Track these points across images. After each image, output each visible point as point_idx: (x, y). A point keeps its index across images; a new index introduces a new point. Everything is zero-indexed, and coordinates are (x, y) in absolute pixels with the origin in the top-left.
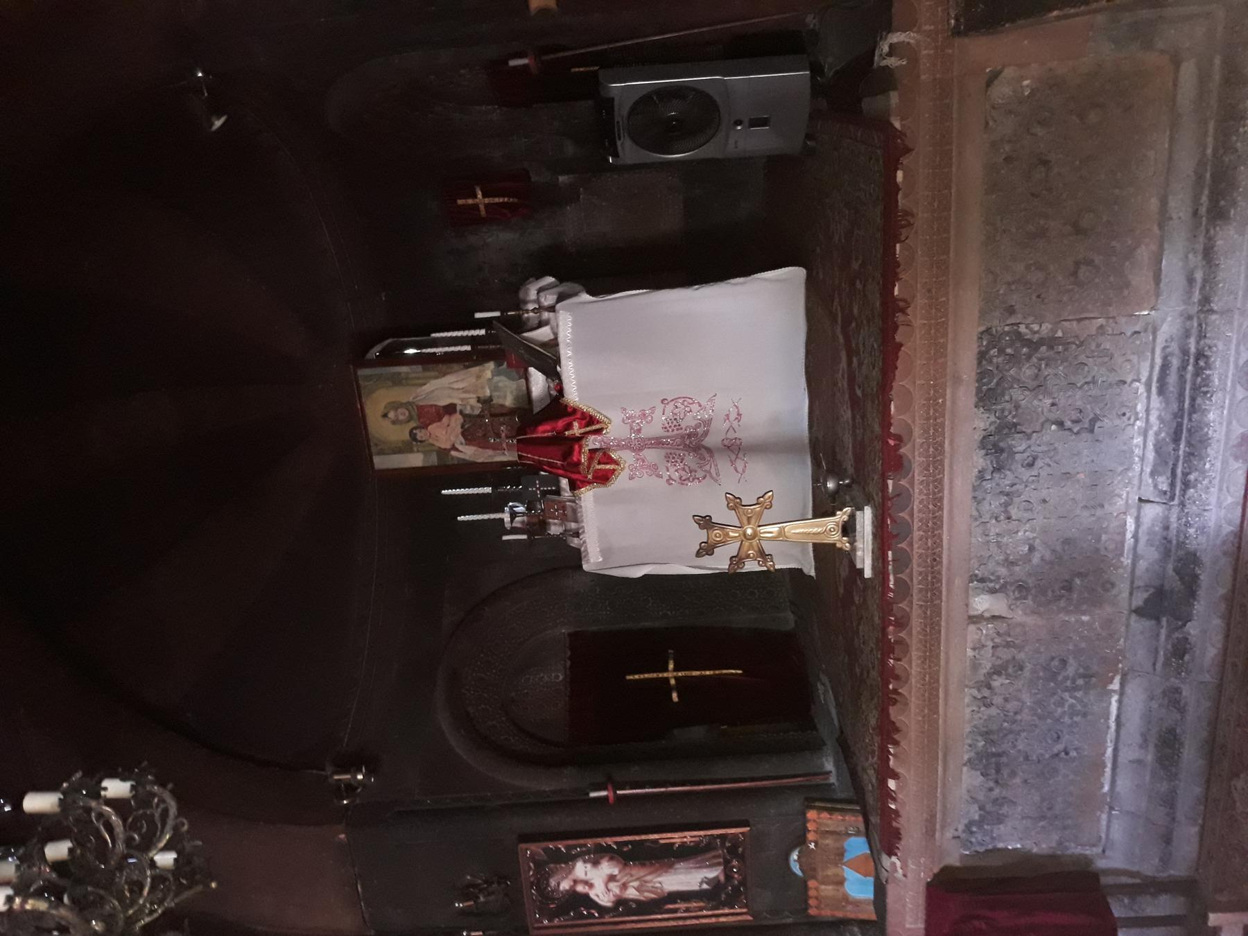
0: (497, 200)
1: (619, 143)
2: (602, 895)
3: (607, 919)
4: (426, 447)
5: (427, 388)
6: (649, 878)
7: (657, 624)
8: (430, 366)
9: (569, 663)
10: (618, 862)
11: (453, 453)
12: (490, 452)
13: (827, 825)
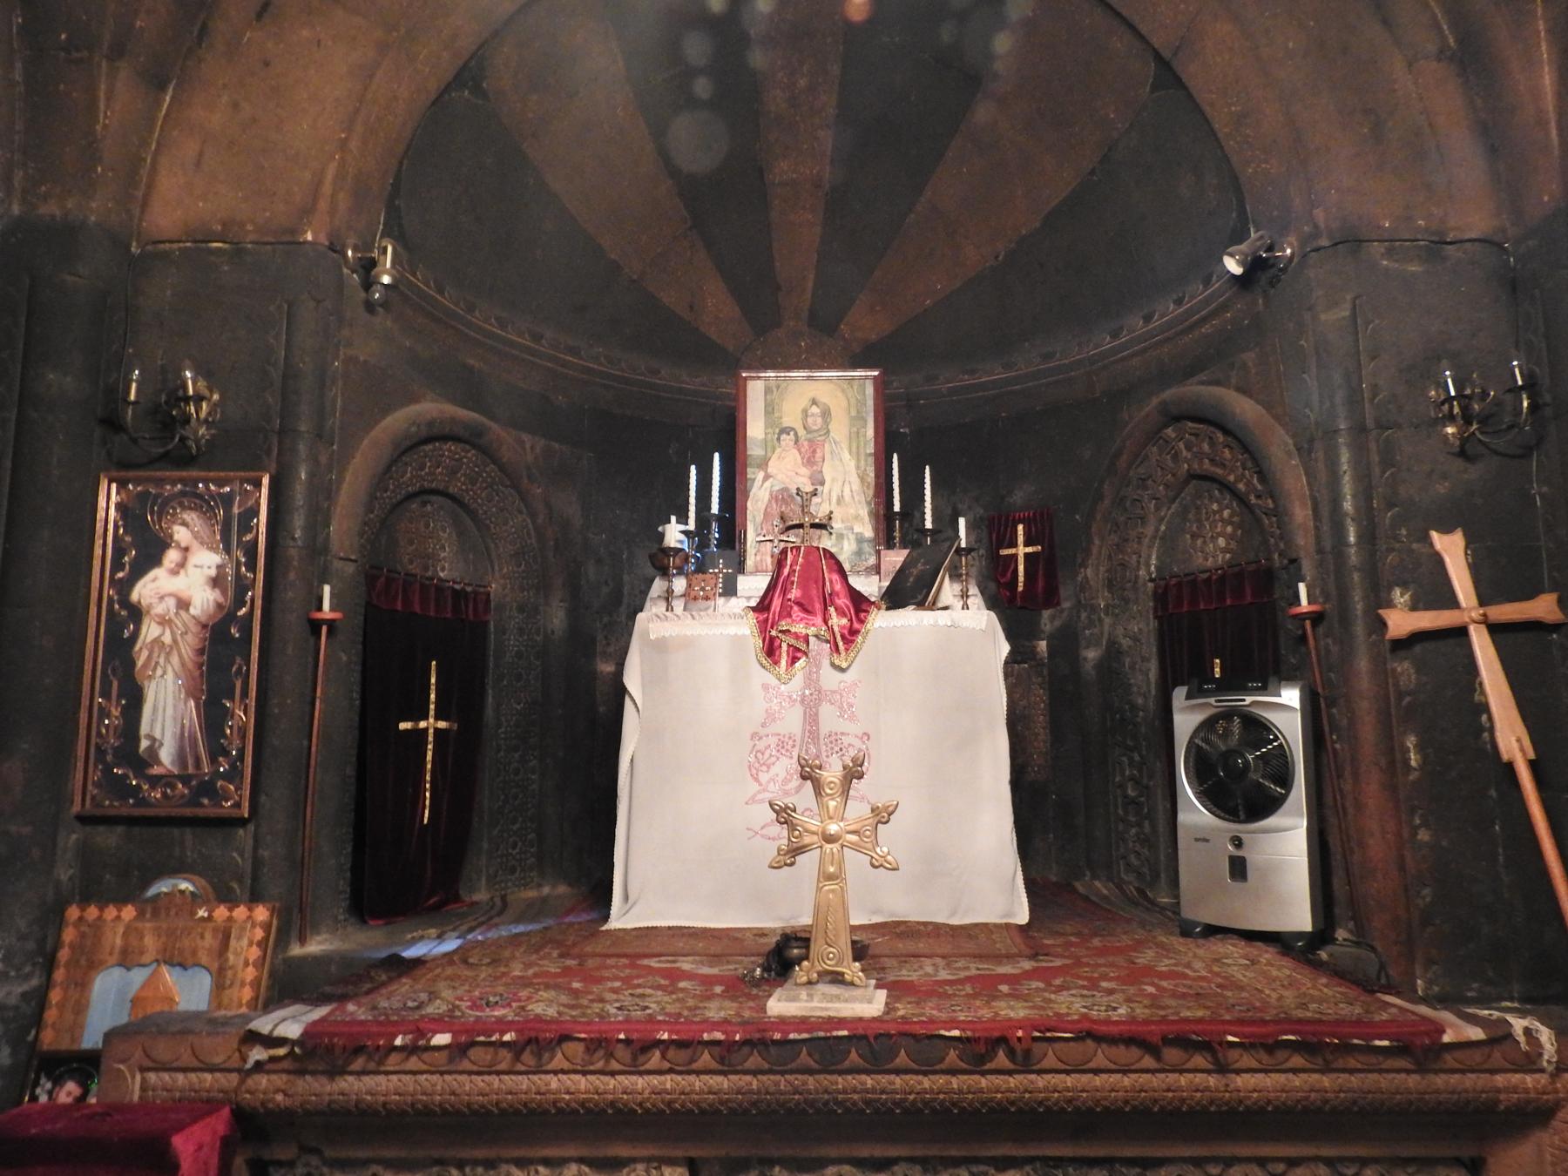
0: (1021, 568)
1: (1212, 700)
2: (153, 588)
3: (109, 592)
4: (769, 446)
5: (846, 456)
6: (175, 659)
7: (489, 712)
8: (871, 460)
9: (457, 587)
10: (210, 617)
11: (761, 475)
12: (760, 518)
13: (239, 938)
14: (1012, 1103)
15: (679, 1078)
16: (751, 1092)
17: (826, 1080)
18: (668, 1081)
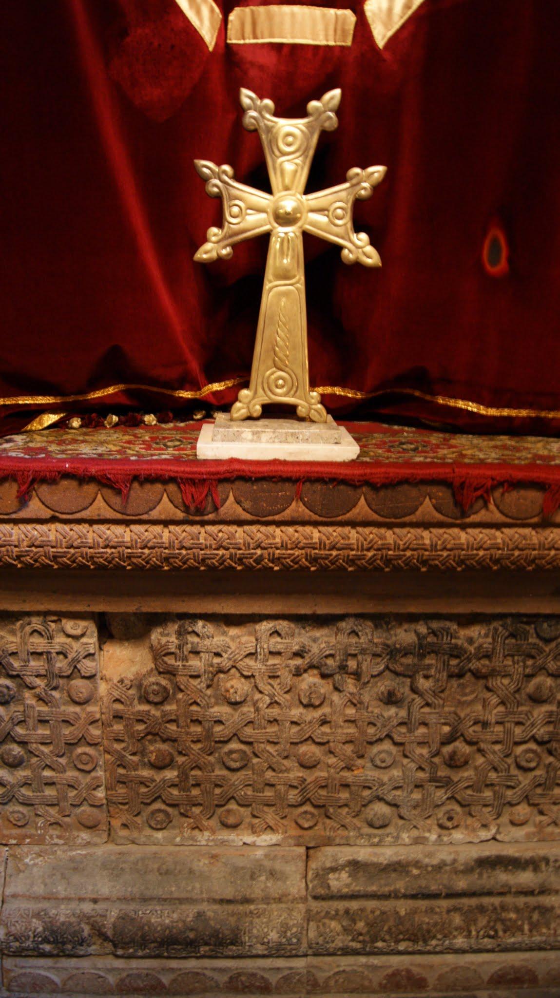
14: (497, 561)
15: (67, 528)
16: (161, 546)
17: (258, 532)
18: (52, 532)
